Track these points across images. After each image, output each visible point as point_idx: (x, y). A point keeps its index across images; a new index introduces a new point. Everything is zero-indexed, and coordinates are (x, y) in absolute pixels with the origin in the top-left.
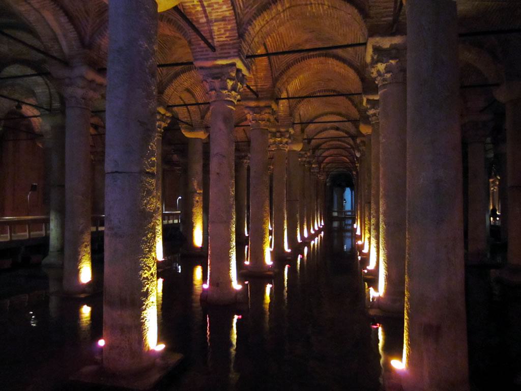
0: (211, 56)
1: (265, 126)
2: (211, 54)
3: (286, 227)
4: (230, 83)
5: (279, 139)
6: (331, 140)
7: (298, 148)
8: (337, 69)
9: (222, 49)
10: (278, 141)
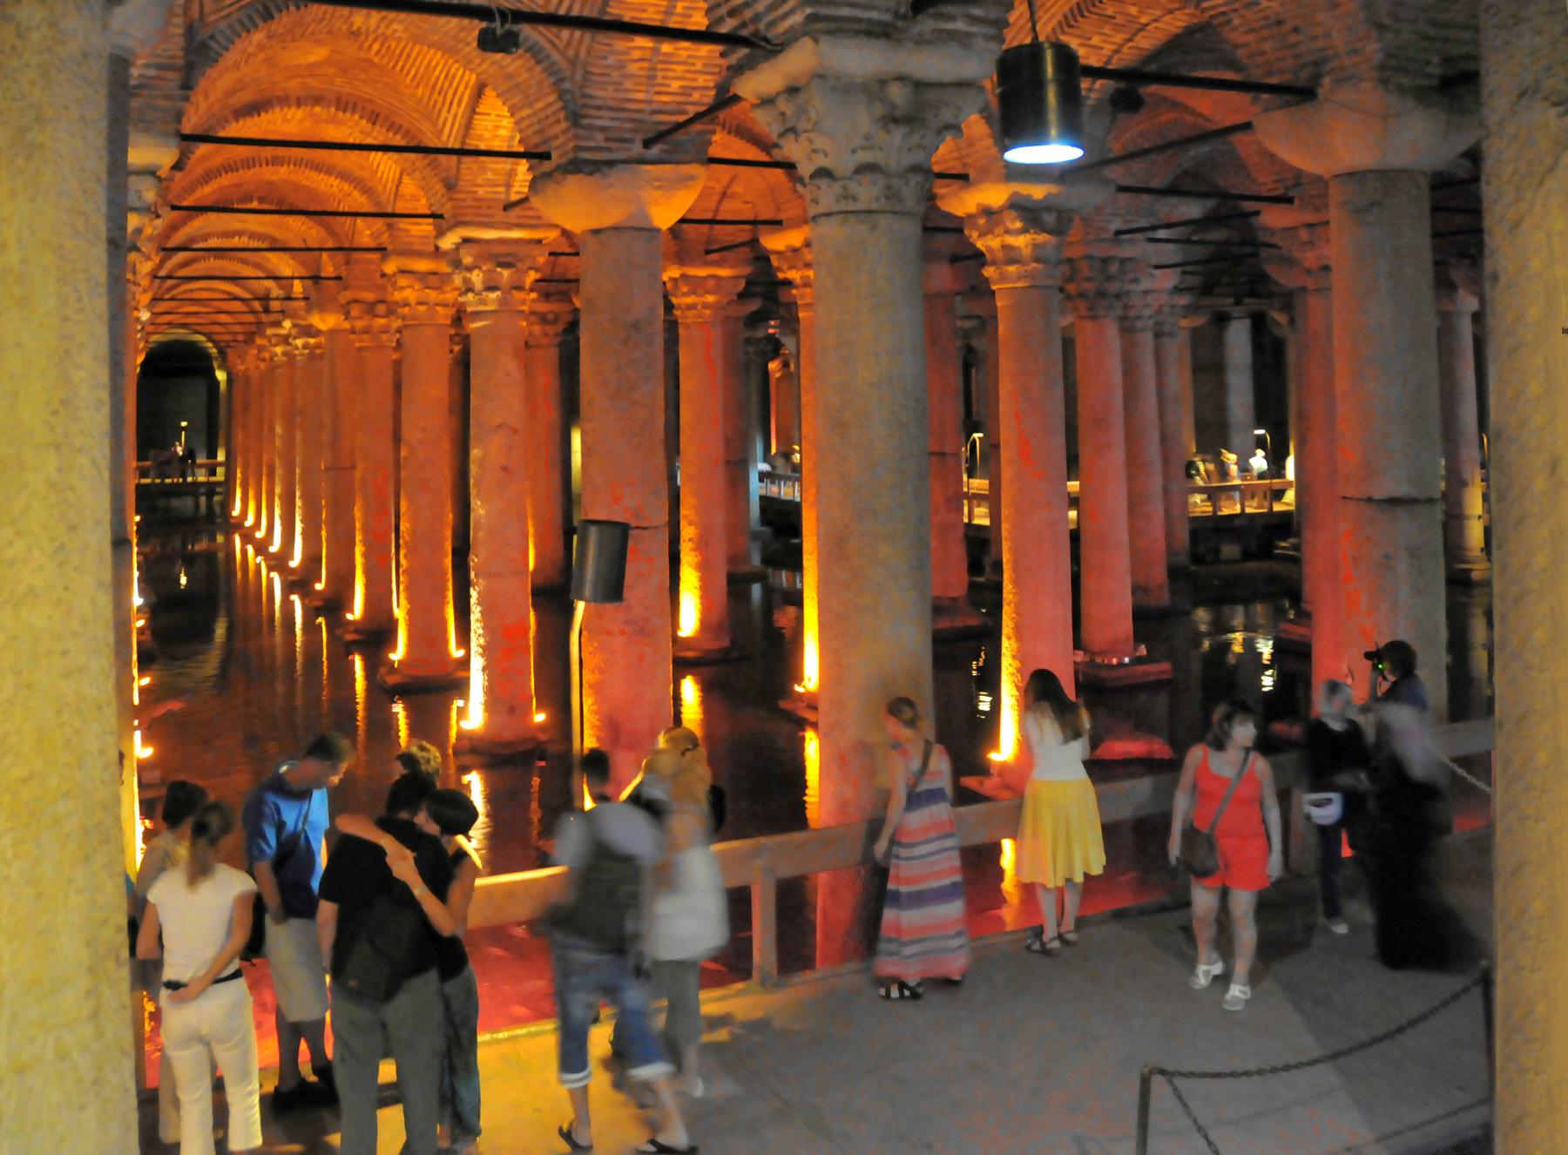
2: (500, 216)
5: (382, 321)
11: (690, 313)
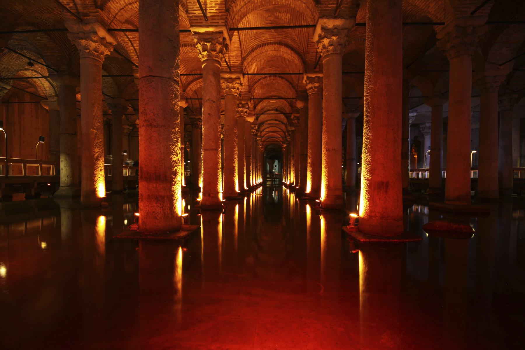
0: (204, 24)
1: (236, 93)
2: (204, 23)
3: (245, 171)
4: (218, 47)
5: (241, 109)
6: (270, 120)
7: (251, 120)
8: (285, 56)
9: (213, 19)
11: (310, 90)
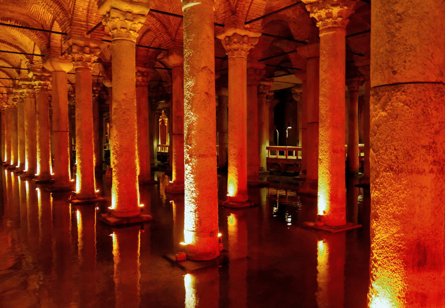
5: (88, 56)
10: (87, 58)
